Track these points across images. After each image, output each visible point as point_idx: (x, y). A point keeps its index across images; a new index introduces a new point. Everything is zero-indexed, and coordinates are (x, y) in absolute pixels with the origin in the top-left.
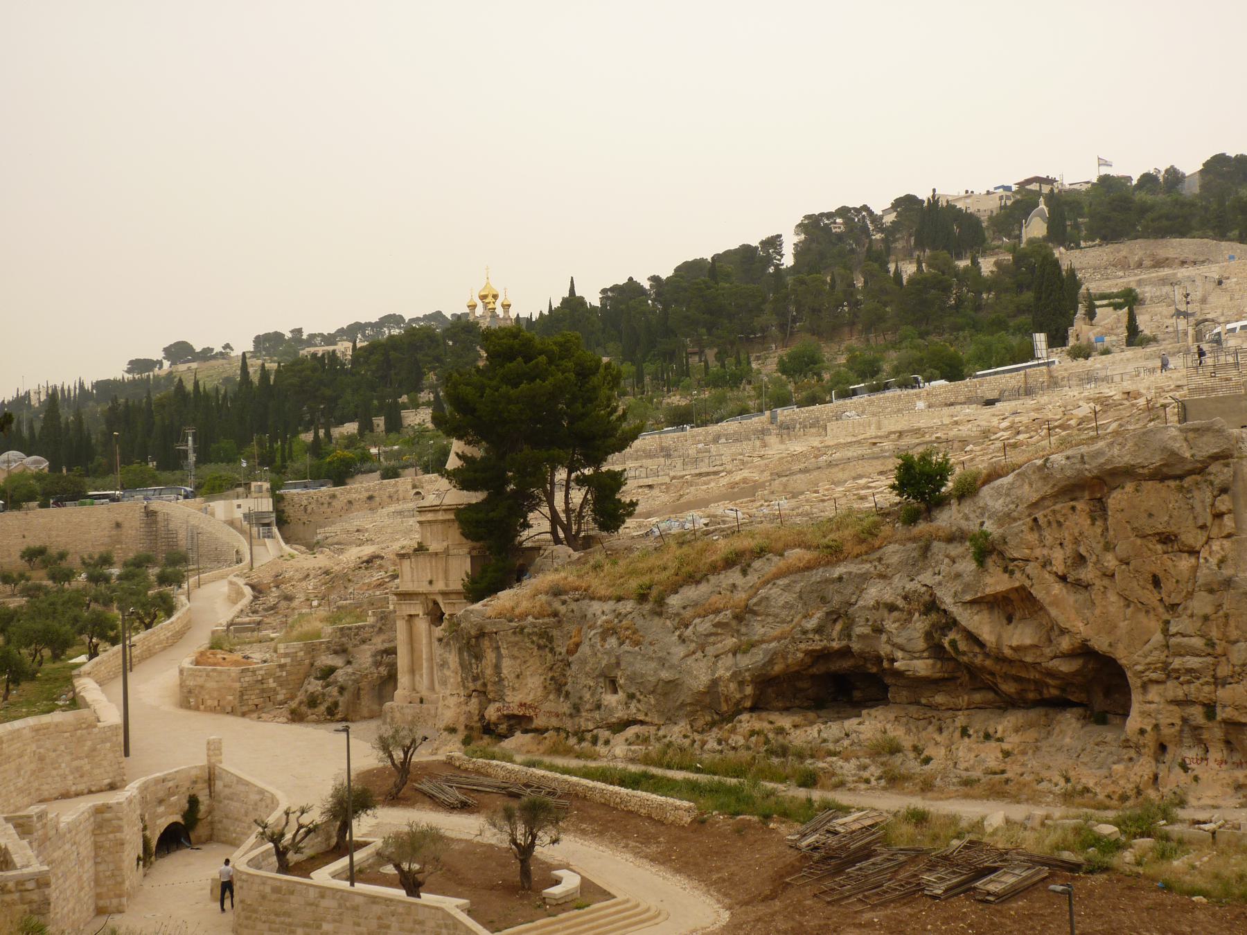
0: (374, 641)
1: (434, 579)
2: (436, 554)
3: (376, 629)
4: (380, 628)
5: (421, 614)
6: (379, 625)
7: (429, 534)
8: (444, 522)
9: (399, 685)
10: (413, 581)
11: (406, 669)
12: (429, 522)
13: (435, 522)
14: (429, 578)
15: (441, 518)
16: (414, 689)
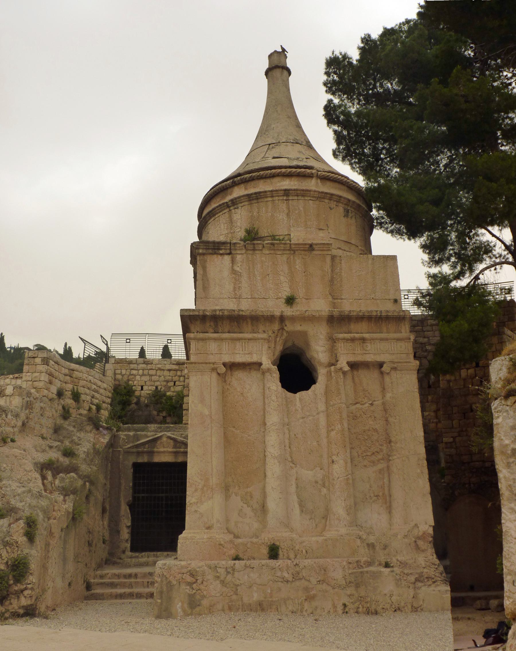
0: (20, 441)
1: (300, 293)
2: (311, 247)
3: (20, 423)
4: (24, 424)
5: (267, 362)
6: (23, 416)
7: (281, 216)
8: (322, 196)
9: (189, 519)
10: (238, 298)
11: (214, 481)
12: (287, 193)
13: (303, 193)
14: (286, 292)
15: (313, 188)
16: (229, 531)
